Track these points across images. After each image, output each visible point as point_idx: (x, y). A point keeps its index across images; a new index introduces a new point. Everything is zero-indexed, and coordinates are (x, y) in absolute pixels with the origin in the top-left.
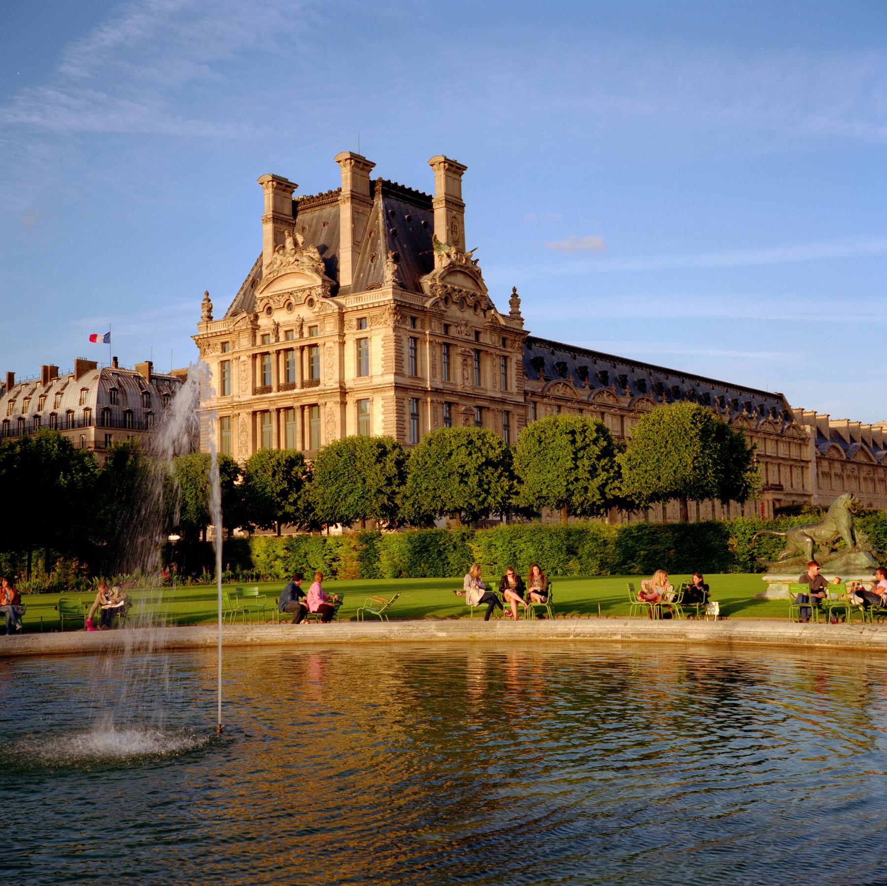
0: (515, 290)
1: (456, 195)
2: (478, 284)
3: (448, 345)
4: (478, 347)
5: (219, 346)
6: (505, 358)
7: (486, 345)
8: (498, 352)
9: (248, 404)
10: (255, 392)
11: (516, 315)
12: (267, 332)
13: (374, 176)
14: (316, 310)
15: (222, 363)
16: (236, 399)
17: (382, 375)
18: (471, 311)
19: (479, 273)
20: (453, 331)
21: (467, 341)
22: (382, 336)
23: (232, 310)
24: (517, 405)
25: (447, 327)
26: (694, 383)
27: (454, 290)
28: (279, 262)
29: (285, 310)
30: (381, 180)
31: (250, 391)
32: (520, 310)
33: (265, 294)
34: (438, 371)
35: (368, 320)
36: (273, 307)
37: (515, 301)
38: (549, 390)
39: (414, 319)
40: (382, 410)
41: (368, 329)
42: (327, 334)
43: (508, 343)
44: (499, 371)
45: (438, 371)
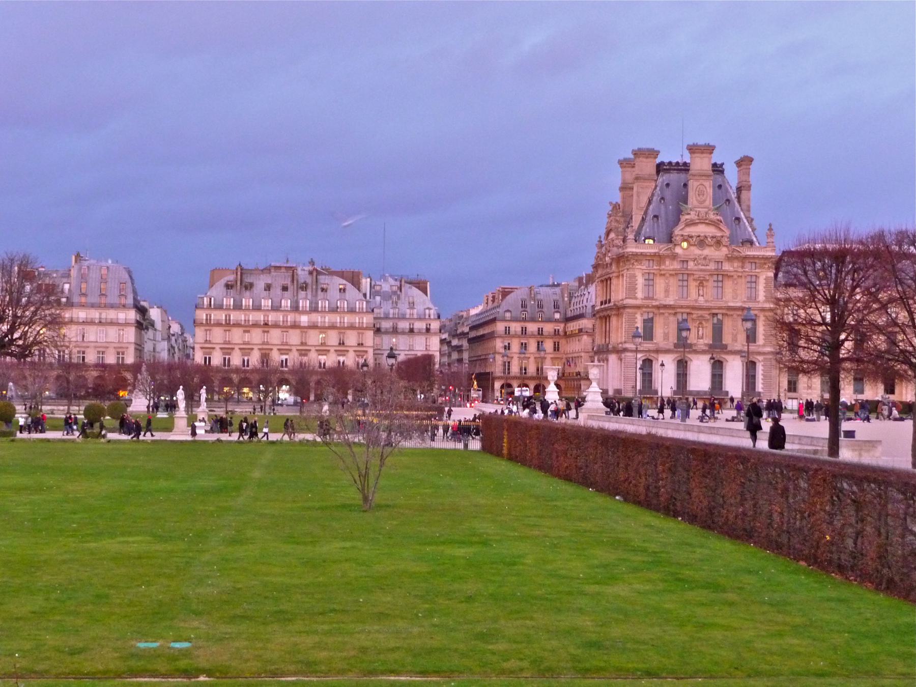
0: (770, 225)
24: (763, 310)
27: (692, 237)
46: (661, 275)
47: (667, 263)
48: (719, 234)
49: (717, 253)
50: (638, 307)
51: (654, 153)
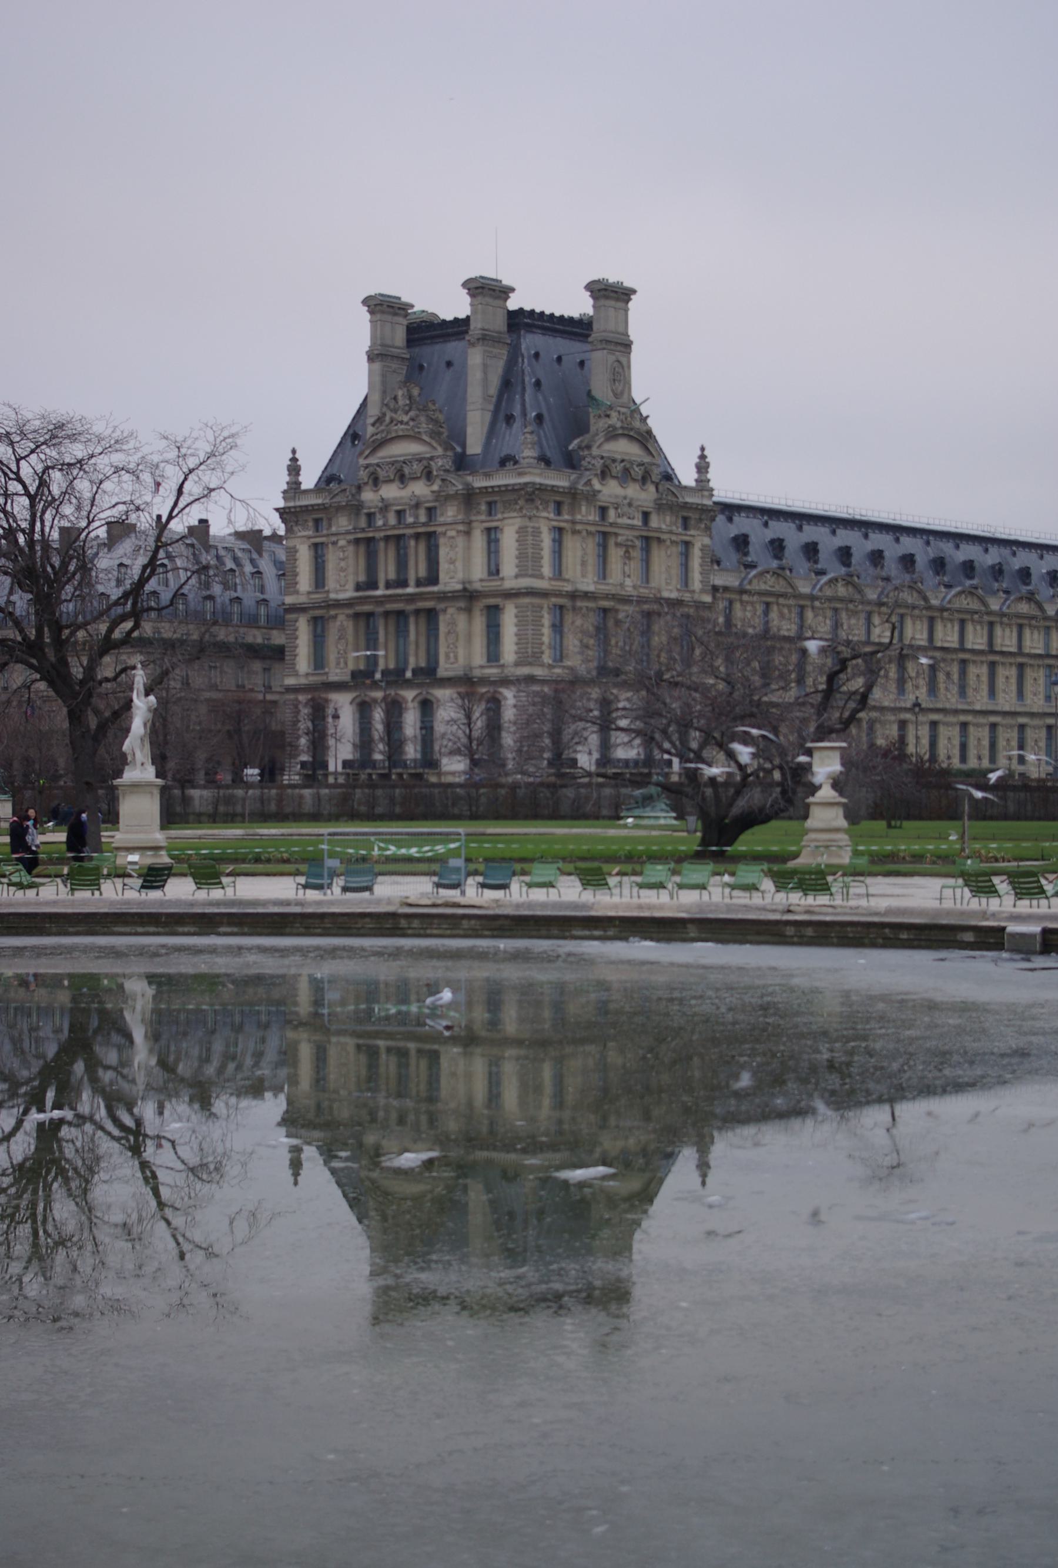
1: (621, 329)
2: (647, 449)
3: (605, 534)
4: (645, 534)
5: (311, 524)
6: (687, 544)
7: (658, 530)
8: (674, 538)
9: (349, 603)
10: (358, 587)
11: (703, 484)
12: (373, 510)
13: (513, 304)
14: (435, 487)
15: (316, 546)
16: (332, 596)
17: (517, 577)
18: (637, 486)
19: (649, 432)
20: (612, 514)
21: (632, 527)
22: (516, 527)
23: (326, 474)
25: (603, 510)
26: (1006, 552)
27: (614, 461)
28: (387, 419)
29: (397, 483)
30: (521, 311)
31: (350, 586)
32: (709, 476)
33: (373, 460)
34: (590, 568)
35: (499, 505)
36: (381, 478)
37: (702, 466)
38: (750, 583)
39: (559, 505)
40: (515, 620)
41: (499, 516)
42: (449, 520)
43: (693, 522)
44: (675, 562)
45: (590, 568)
46: (575, 532)
47: (584, 509)
48: (647, 459)
49: (643, 495)
50: (544, 594)
51: (505, 292)
